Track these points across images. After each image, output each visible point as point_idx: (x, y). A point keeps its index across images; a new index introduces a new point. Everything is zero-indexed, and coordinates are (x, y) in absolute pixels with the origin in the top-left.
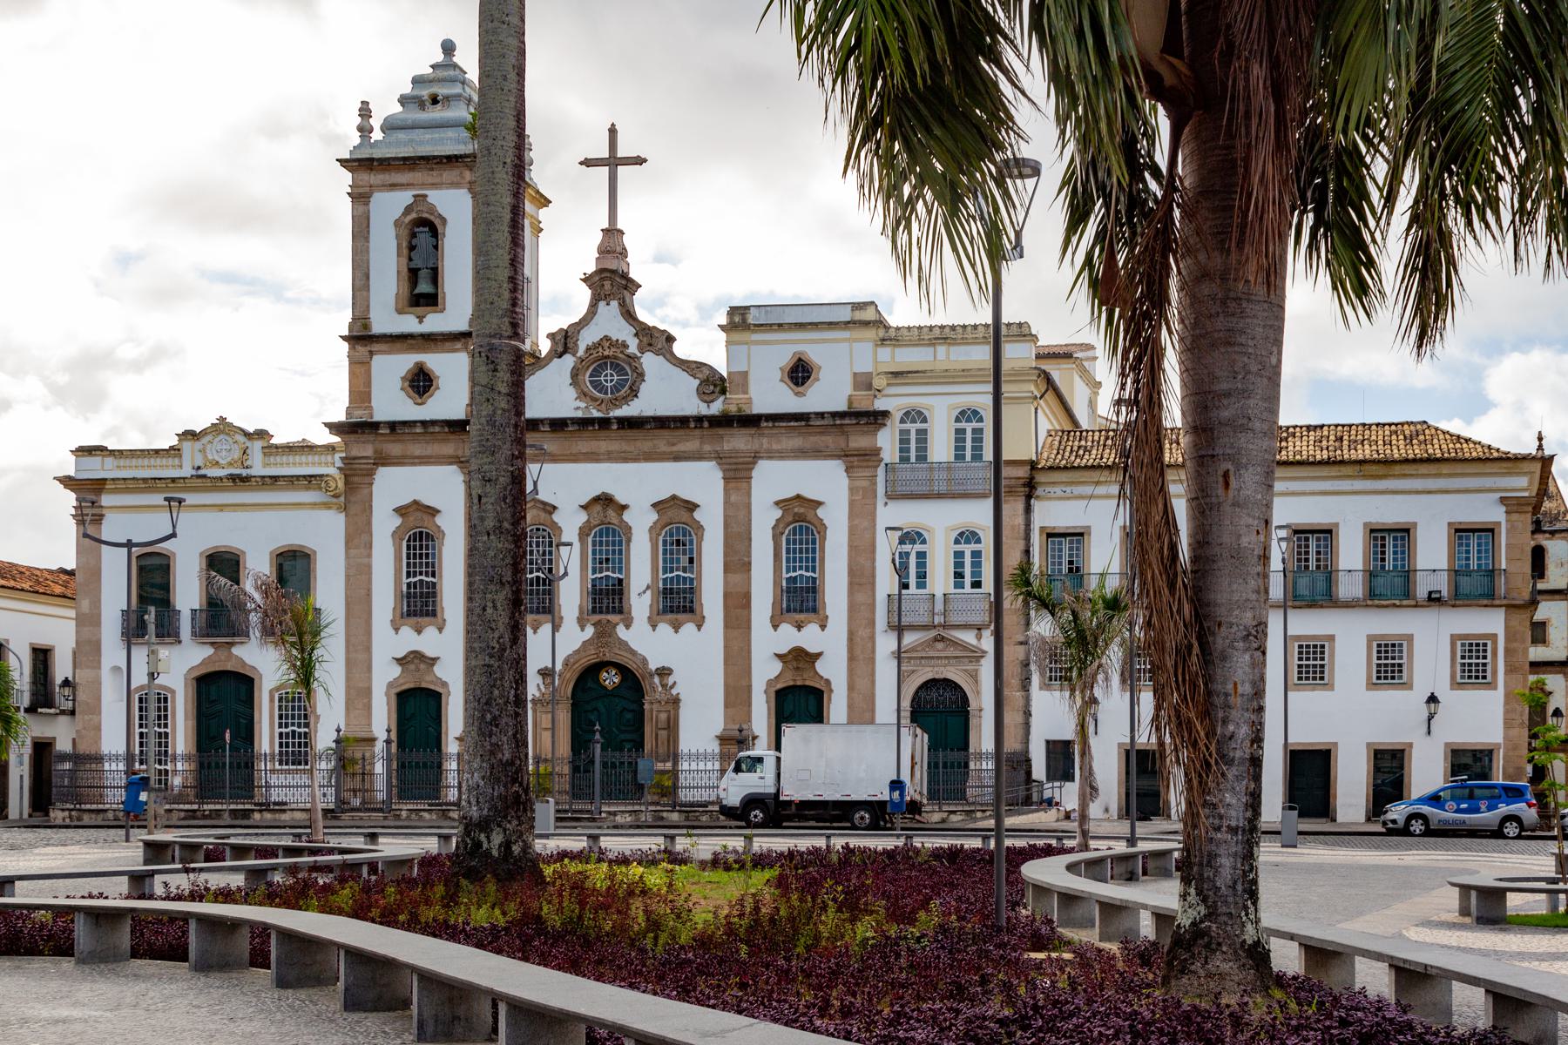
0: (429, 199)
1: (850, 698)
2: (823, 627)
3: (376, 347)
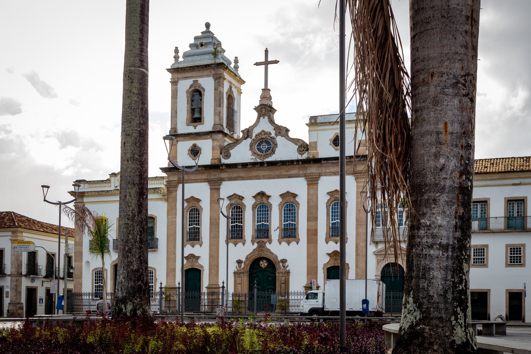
0: (199, 82)
1: (356, 271)
3: (179, 139)
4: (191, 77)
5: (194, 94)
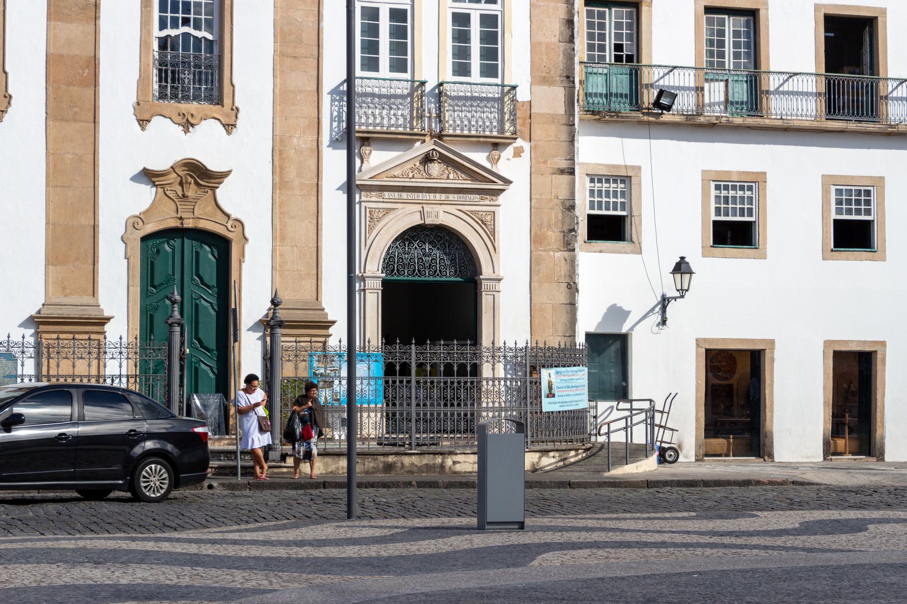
2: (229, 127)
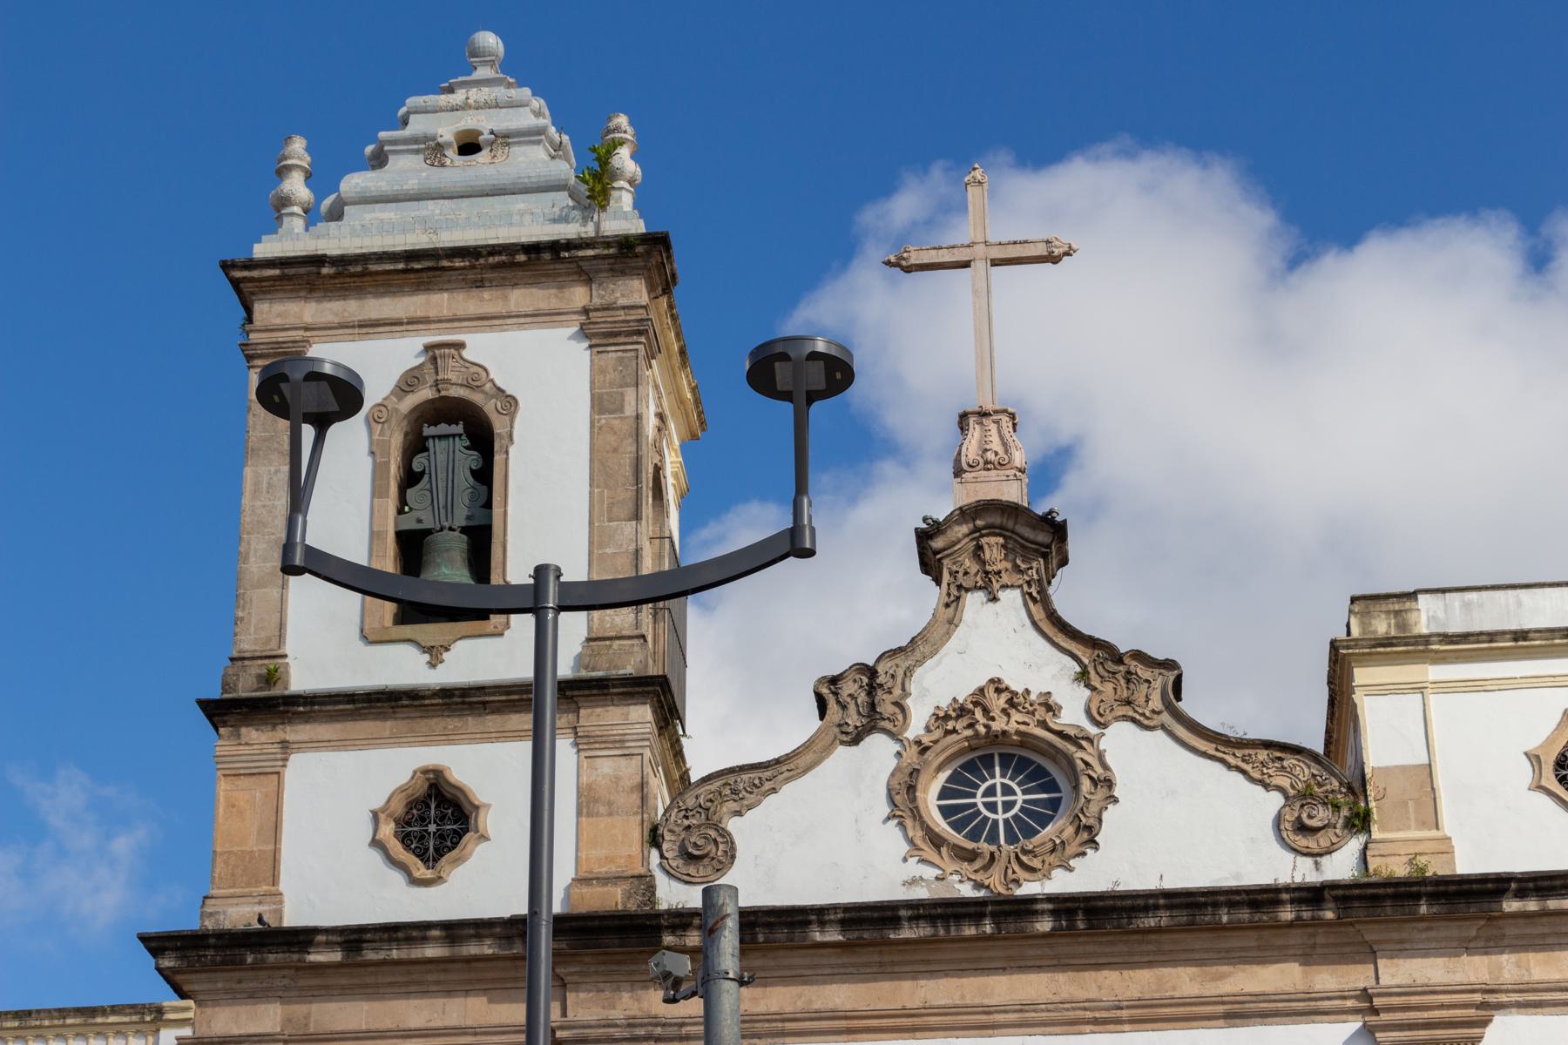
4: (412, 321)
5: (428, 431)
